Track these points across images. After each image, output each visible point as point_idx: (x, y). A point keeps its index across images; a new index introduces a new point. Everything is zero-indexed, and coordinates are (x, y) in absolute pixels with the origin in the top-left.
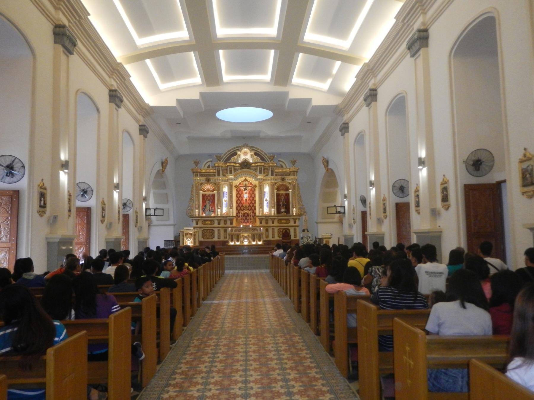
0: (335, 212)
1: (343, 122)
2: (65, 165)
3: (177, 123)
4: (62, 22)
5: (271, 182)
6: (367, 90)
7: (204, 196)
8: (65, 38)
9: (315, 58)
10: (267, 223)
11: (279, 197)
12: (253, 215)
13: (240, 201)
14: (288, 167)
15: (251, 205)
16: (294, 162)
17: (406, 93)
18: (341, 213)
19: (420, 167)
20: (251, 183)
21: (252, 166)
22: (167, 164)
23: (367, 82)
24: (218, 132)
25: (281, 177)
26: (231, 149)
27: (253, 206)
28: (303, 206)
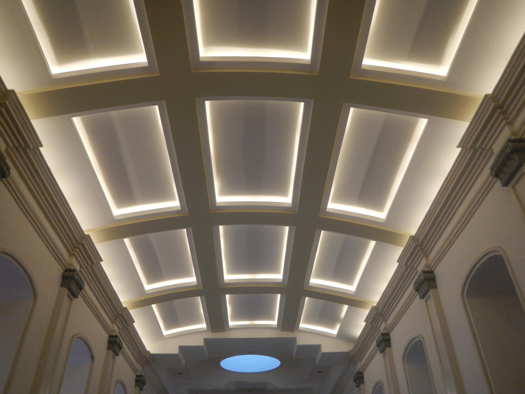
4: (73, 267)
6: (379, 335)
8: (73, 282)
9: (321, 302)
17: (422, 337)
23: (378, 326)
24: (221, 384)
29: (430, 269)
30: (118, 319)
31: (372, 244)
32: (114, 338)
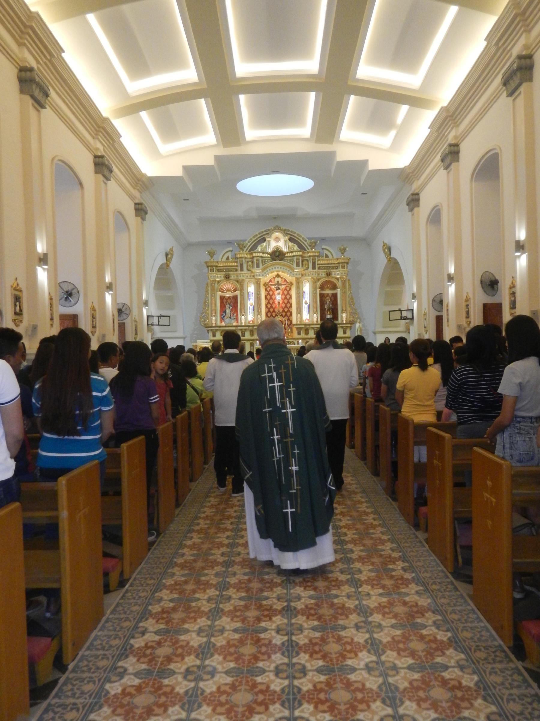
2: (43, 260)
4: (29, 64)
5: (313, 278)
7: (222, 298)
8: (34, 86)
9: (372, 101)
10: (307, 332)
12: (289, 323)
13: (271, 305)
14: (335, 257)
15: (286, 310)
17: (501, 150)
18: (408, 319)
19: (518, 254)
20: (285, 280)
21: (287, 257)
22: (172, 255)
24: (239, 211)
25: (325, 271)
26: (257, 233)
27: (289, 311)
28: (355, 310)
29: (529, 52)
30: (100, 134)
31: (453, 10)
32: (101, 159)
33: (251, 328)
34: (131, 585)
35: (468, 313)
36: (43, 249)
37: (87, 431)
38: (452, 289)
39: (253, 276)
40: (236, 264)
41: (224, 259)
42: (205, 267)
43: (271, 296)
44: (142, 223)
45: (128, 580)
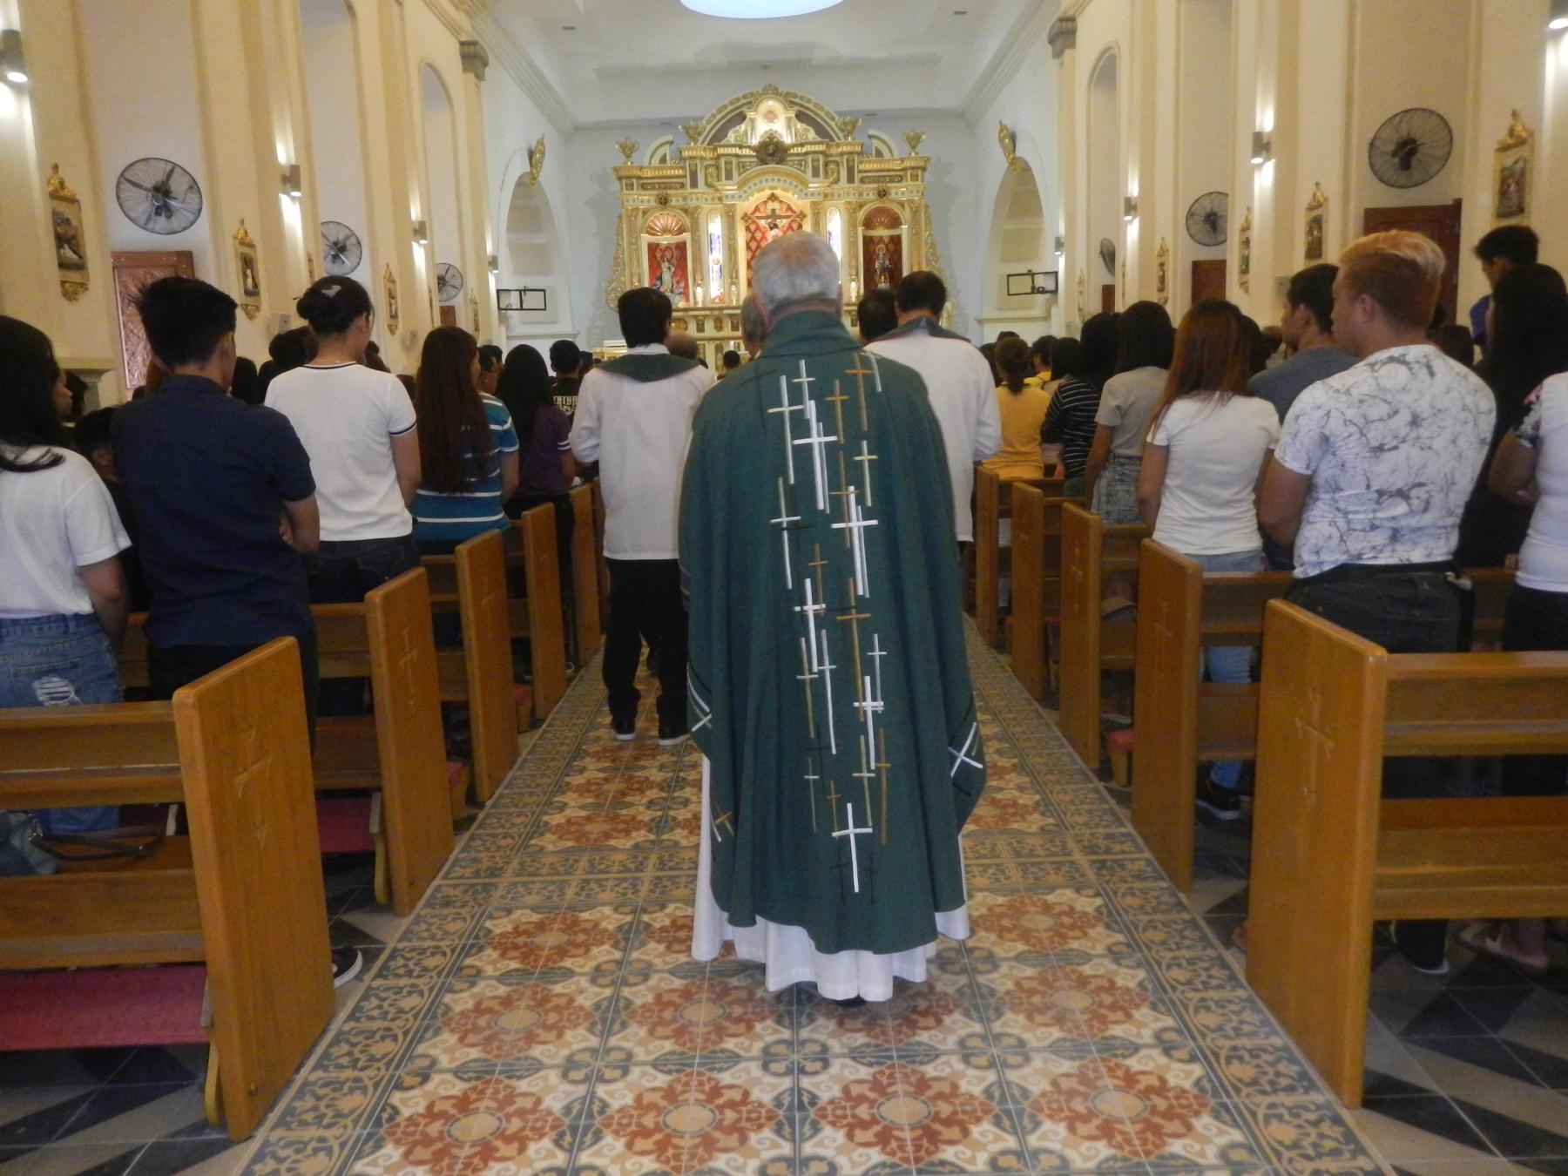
0: (1029, 290)
1: (1058, 15)
2: (291, 179)
3: (565, 28)
5: (849, 203)
7: (653, 248)
11: (871, 247)
14: (896, 155)
16: (914, 141)
20: (789, 208)
21: (792, 155)
22: (543, 154)
24: (686, 52)
25: (875, 185)
26: (726, 102)
33: (716, 313)
34: (549, 725)
35: (1162, 280)
36: (288, 155)
37: (485, 485)
38: (1133, 231)
39: (720, 199)
40: (681, 172)
41: (655, 162)
42: (614, 177)
43: (759, 243)
44: (478, 87)
45: (543, 720)
